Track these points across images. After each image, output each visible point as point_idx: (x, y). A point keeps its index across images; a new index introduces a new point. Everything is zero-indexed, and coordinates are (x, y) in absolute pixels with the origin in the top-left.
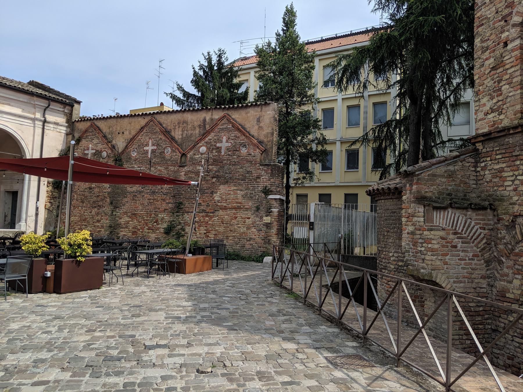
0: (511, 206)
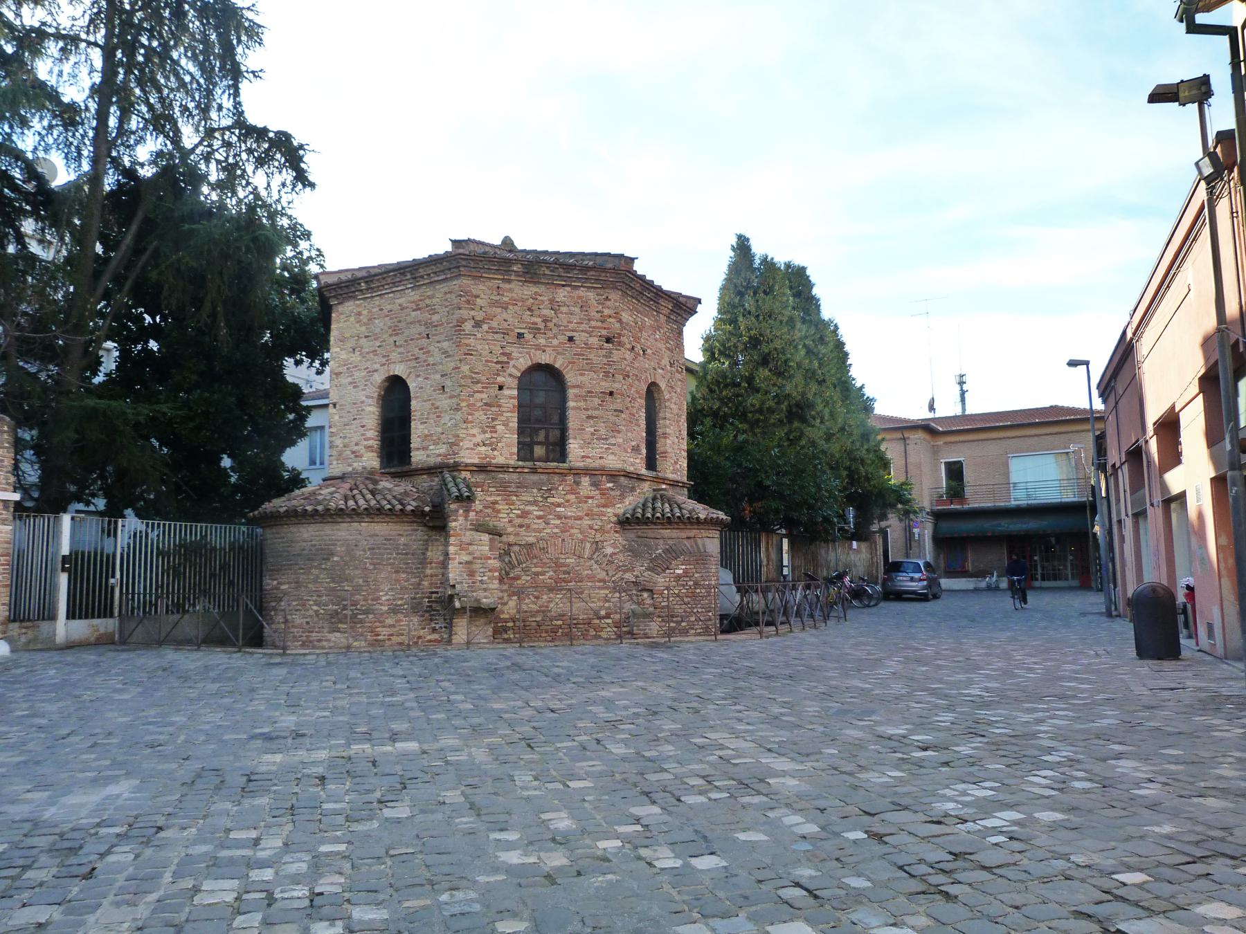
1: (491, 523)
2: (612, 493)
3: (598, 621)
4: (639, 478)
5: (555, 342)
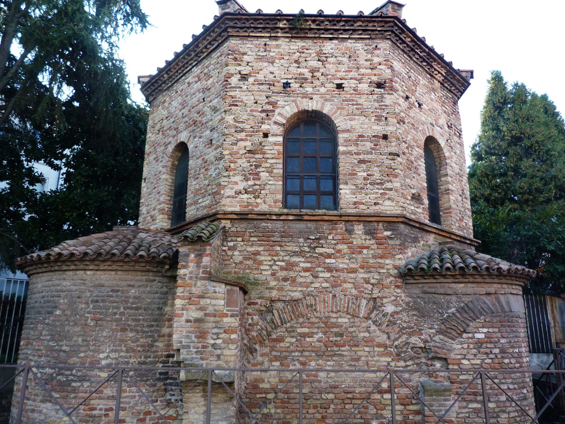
0: (267, 291)
1: (251, 276)
2: (390, 242)
3: (378, 396)
4: (422, 228)
5: (323, 90)
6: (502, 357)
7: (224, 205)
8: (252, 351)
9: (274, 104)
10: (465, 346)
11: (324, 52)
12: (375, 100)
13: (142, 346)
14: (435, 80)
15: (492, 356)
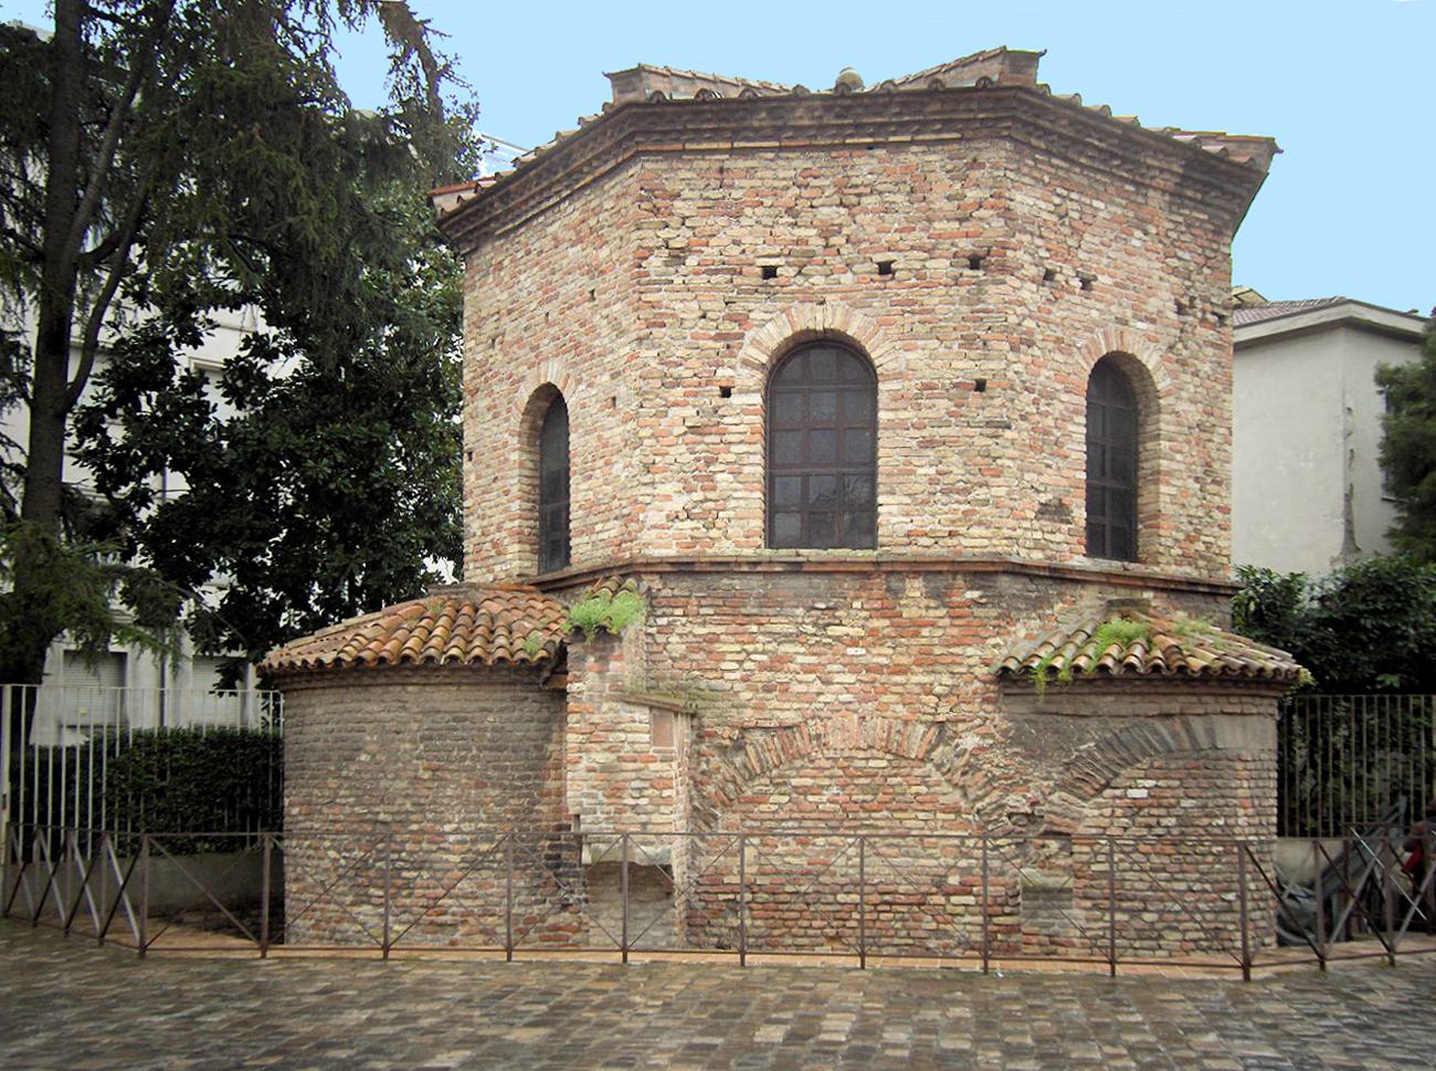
2: (978, 611)
4: (1060, 577)
5: (847, 279)
6: (1182, 833)
7: (646, 545)
8: (709, 819)
9: (742, 320)
10: (1107, 812)
11: (854, 181)
12: (962, 298)
13: (514, 812)
14: (1151, 193)
15: (1159, 831)
